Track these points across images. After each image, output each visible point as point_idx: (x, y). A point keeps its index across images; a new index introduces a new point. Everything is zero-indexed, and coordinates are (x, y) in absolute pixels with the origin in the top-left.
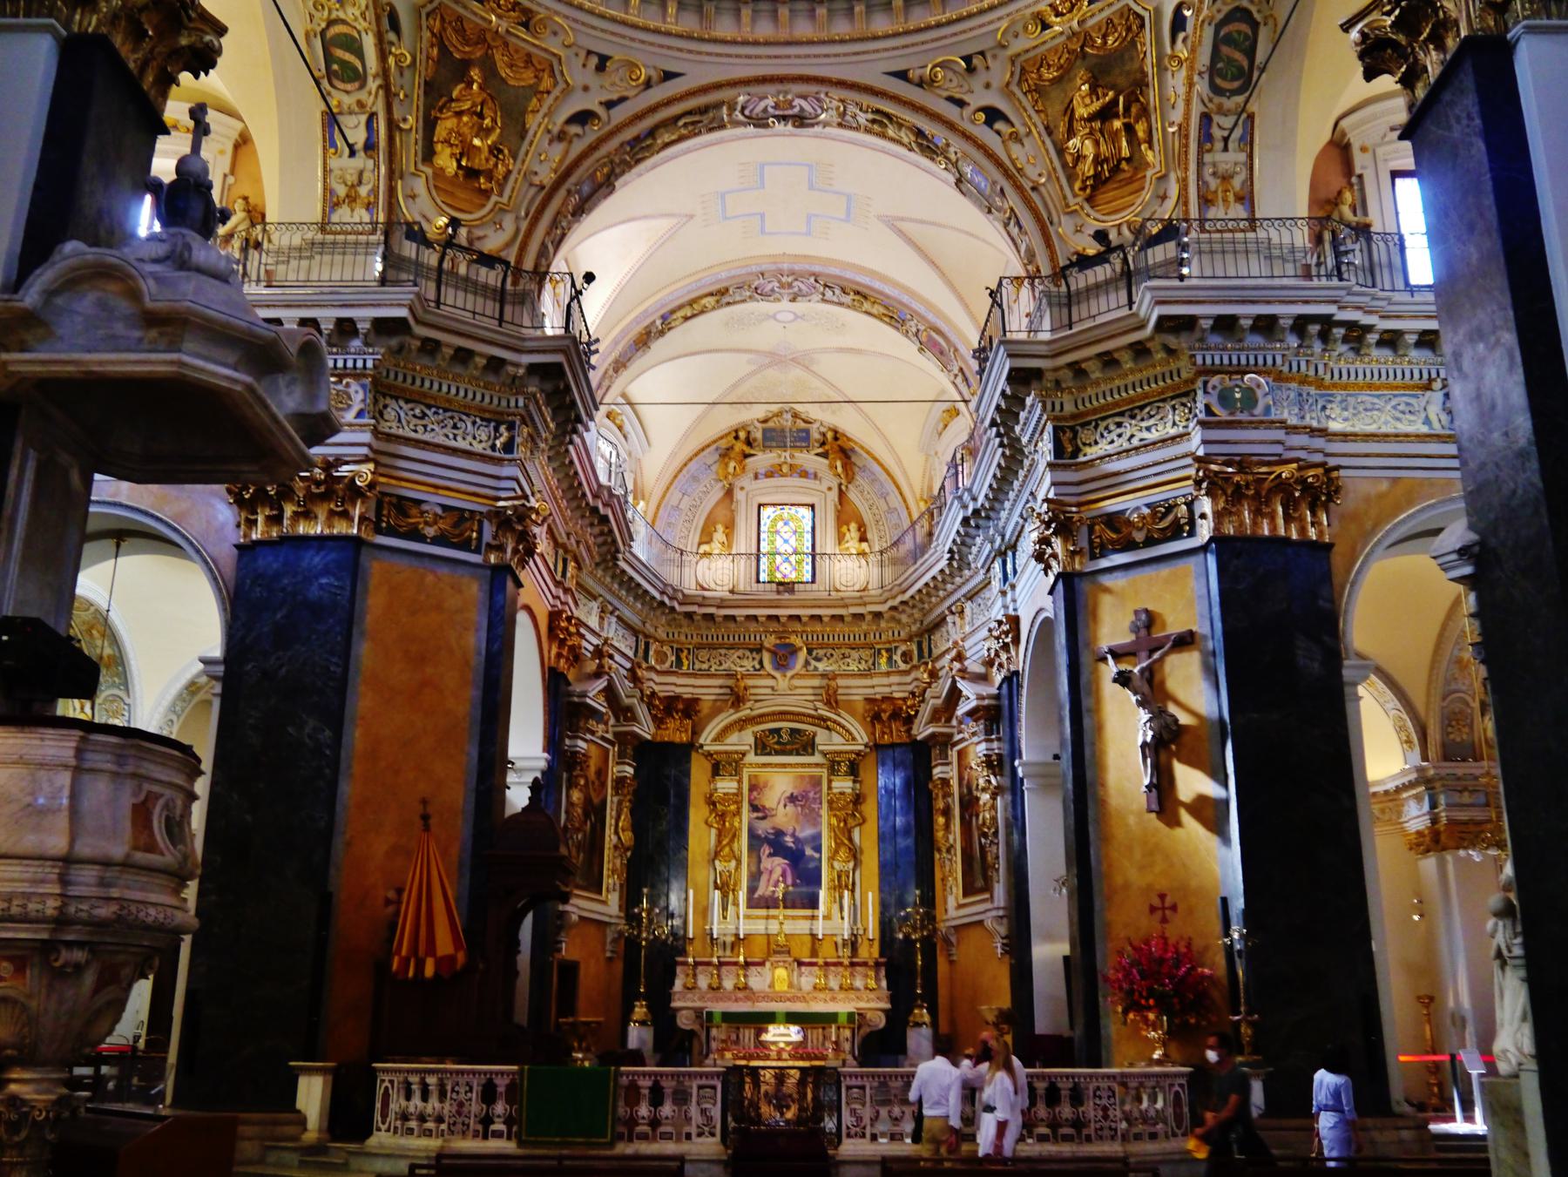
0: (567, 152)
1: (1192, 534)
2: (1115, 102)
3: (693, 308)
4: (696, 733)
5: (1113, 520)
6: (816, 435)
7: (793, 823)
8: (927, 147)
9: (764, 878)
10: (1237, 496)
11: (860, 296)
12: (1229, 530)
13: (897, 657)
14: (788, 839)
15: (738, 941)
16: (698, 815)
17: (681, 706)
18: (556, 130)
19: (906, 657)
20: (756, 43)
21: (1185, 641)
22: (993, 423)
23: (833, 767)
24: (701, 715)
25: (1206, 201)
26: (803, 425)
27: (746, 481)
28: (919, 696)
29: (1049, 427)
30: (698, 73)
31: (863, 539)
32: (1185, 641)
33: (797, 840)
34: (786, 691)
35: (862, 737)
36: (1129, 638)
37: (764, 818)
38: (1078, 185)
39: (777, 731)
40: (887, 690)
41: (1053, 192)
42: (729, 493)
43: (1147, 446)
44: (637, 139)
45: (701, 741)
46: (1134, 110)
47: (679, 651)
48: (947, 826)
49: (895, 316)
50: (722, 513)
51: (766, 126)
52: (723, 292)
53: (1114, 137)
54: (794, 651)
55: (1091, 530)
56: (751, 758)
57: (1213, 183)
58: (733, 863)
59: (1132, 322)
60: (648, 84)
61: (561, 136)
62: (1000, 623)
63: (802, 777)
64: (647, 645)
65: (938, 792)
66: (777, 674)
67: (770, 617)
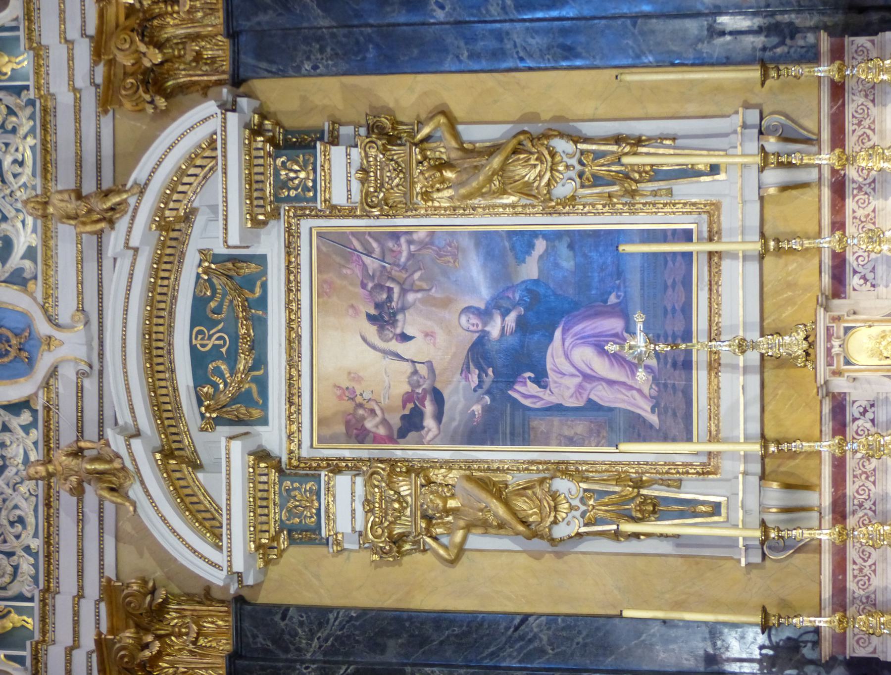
4: (207, 595)
7: (450, 315)
9: (603, 395)
14: (494, 330)
16: (429, 586)
17: (128, 636)
23: (305, 202)
24: (159, 574)
33: (498, 305)
37: (438, 398)
39: (199, 360)
40: (83, 50)
45: (217, 578)
56: (272, 436)
58: (562, 485)
63: (325, 290)
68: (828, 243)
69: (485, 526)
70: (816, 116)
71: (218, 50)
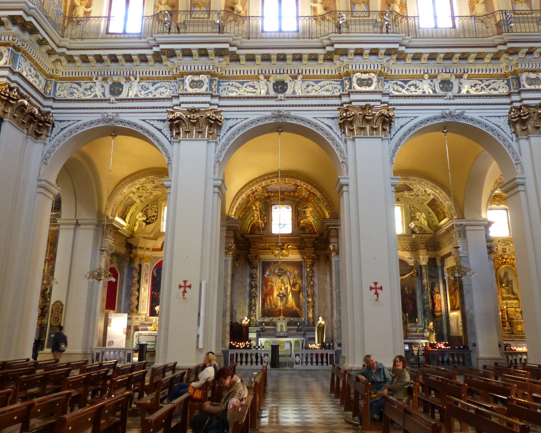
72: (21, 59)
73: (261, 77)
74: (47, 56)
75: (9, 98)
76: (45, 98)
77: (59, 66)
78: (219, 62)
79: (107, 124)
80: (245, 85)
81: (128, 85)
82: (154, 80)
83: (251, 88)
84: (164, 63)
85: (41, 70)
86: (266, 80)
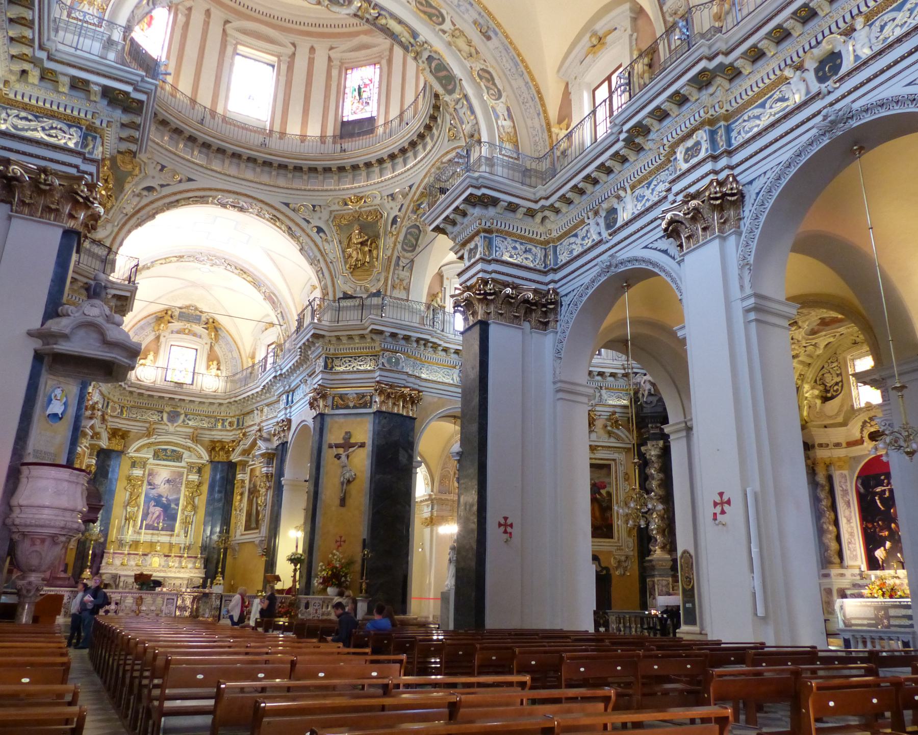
0: (139, 203)
1: (370, 407)
2: (367, 240)
3: (166, 260)
4: (126, 447)
5: (341, 397)
6: (204, 319)
8: (292, 235)
9: (150, 516)
10: (388, 396)
11: (243, 272)
12: (384, 409)
13: (226, 424)
15: (136, 544)
18: (137, 192)
19: (231, 424)
20: (229, 176)
21: (362, 445)
22: (300, 348)
23: (190, 470)
25: (394, 287)
26: (198, 313)
27: (166, 333)
28: (236, 442)
29: (324, 356)
30: (203, 182)
31: (218, 369)
32: (362, 445)
34: (174, 433)
35: (206, 456)
36: (342, 442)
38: (348, 266)
39: (166, 450)
41: (340, 266)
42: (158, 338)
43: (359, 372)
44: (172, 202)
46: (374, 245)
47: (123, 407)
48: (241, 500)
49: (256, 283)
50: (153, 346)
51: (226, 207)
52: (181, 257)
53: (364, 254)
54: (178, 414)
55: (334, 398)
56: (151, 461)
57: (397, 281)
59: (362, 327)
60: (180, 181)
61: (139, 195)
62: (283, 421)
64: (108, 403)
65: (237, 484)
66: (169, 424)
67: (170, 398)
68: (173, 555)
69: (131, 494)
70: (192, 554)
71: (216, 459)
72: (497, 241)
73: (788, 72)
74: (530, 219)
75: (486, 294)
76: (545, 273)
77: (548, 225)
78: (712, 95)
79: (608, 275)
80: (767, 106)
81: (622, 204)
82: (645, 180)
83: (779, 104)
84: (646, 148)
85: (531, 240)
86: (798, 73)
